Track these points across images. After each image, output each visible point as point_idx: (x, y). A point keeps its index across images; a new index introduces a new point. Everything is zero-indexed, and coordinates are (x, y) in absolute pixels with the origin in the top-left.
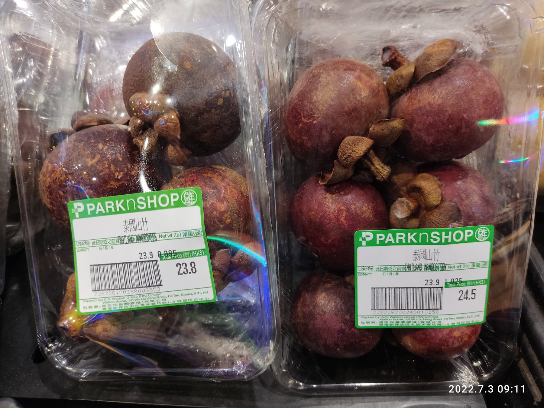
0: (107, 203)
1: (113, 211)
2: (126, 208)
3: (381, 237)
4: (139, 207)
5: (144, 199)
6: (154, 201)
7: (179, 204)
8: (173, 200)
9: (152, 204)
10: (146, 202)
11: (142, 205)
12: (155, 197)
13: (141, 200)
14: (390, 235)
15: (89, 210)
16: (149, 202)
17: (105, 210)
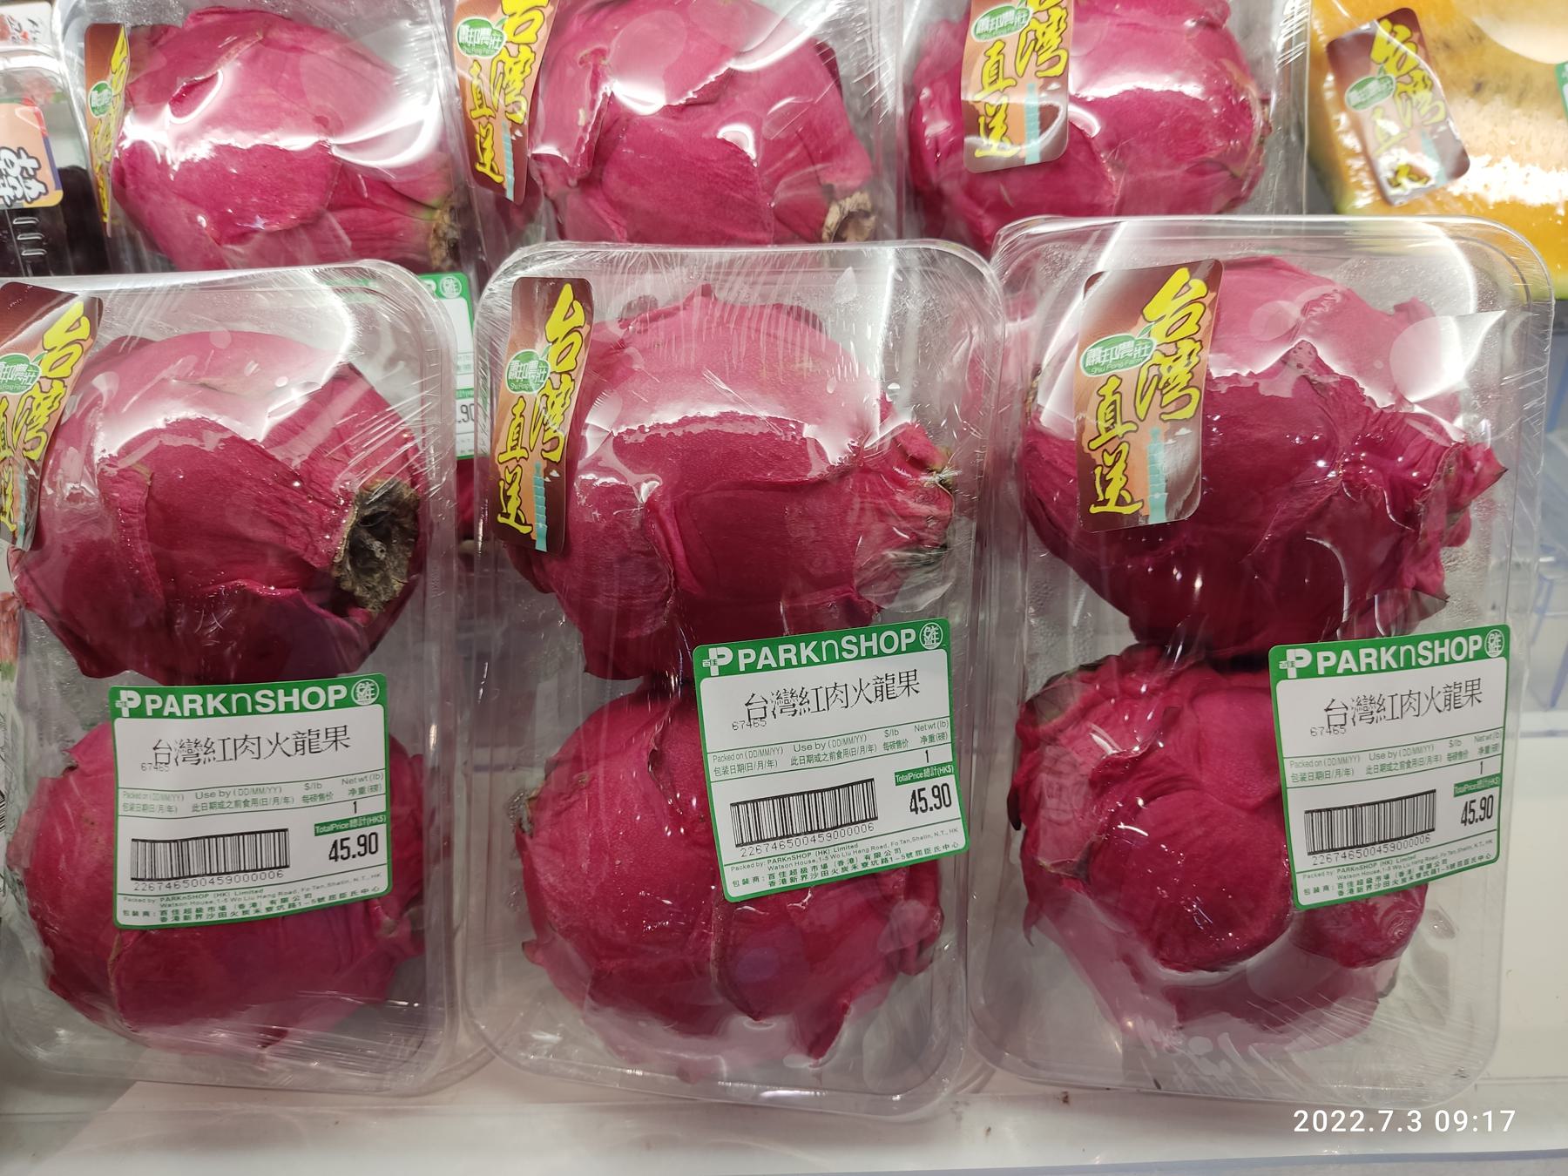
0: (781, 648)
1: (794, 662)
2: (820, 657)
3: (1327, 659)
4: (845, 654)
5: (854, 640)
6: (873, 643)
7: (915, 647)
8: (904, 641)
9: (869, 649)
10: (858, 644)
11: (851, 652)
12: (874, 635)
13: (849, 642)
14: (1347, 654)
15: (742, 662)
16: (864, 644)
17: (777, 662)
